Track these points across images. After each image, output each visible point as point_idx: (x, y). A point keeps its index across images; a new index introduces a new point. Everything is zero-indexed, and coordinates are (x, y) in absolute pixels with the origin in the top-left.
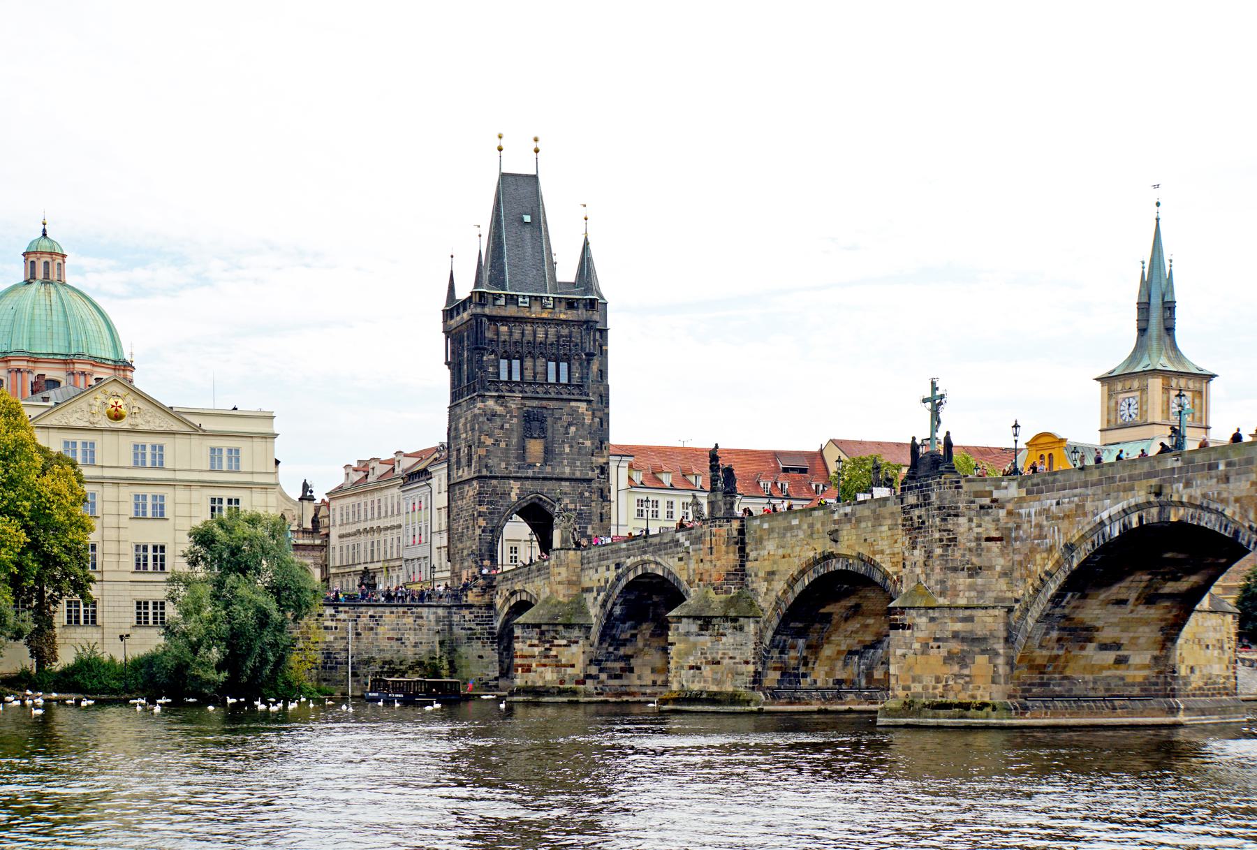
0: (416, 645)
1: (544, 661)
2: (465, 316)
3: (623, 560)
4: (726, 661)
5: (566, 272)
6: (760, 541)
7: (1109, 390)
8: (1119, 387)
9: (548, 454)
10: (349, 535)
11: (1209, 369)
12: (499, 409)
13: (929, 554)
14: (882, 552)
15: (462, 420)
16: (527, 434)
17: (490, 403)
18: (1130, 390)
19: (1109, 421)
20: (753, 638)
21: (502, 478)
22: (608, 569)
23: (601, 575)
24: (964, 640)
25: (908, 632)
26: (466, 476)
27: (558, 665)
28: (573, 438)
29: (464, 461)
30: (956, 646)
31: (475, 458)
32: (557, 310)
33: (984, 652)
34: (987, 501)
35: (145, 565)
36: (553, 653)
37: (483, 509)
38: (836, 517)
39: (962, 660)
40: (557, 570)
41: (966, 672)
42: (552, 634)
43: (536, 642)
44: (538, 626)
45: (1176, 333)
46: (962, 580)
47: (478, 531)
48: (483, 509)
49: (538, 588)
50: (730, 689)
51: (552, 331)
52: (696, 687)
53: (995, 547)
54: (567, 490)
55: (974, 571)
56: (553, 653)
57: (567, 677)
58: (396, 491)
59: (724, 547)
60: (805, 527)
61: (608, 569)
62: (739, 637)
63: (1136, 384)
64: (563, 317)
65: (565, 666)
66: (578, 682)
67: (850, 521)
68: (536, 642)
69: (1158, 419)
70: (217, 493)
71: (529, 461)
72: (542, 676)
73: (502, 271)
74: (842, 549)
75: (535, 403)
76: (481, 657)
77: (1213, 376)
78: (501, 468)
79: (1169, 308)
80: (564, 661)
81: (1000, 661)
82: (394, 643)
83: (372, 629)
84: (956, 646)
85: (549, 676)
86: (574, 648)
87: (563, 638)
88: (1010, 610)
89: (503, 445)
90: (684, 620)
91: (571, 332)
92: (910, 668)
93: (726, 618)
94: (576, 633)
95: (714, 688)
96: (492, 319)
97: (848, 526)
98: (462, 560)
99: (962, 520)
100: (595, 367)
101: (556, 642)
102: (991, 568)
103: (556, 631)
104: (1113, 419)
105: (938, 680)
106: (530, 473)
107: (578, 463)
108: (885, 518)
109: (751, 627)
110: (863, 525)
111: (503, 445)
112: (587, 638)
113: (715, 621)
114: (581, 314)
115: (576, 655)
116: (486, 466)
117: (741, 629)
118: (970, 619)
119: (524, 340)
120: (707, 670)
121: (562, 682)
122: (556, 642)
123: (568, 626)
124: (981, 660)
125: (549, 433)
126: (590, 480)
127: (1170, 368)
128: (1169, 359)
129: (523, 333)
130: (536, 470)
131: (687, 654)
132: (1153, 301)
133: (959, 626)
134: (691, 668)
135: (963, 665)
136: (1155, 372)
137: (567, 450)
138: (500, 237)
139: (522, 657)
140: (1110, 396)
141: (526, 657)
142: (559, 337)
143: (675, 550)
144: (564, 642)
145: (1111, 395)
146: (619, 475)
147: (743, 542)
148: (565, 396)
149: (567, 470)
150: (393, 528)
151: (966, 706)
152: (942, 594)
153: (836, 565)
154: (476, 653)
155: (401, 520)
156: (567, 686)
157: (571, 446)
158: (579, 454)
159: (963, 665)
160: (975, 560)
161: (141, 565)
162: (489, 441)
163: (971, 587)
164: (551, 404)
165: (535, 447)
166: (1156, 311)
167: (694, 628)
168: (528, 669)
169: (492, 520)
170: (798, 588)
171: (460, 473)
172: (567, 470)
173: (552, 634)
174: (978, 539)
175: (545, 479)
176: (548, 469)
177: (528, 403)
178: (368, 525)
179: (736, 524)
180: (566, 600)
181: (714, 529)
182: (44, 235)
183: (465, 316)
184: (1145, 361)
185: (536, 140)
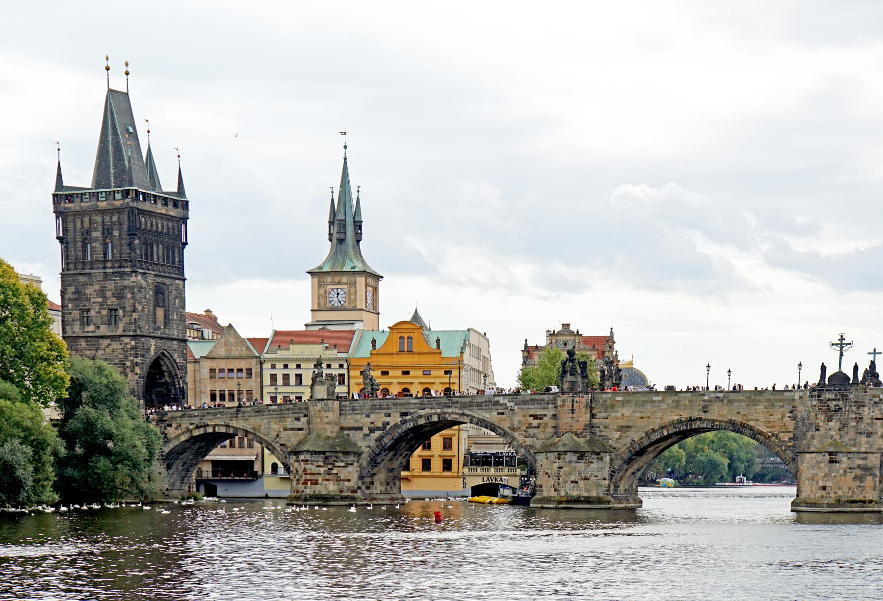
1: (327, 477)
3: (412, 411)
4: (593, 478)
7: (319, 282)
8: (329, 280)
13: (844, 425)
14: (757, 420)
15: (97, 287)
16: (157, 305)
18: (339, 283)
19: (319, 304)
20: (608, 465)
24: (862, 469)
27: (338, 480)
30: (858, 472)
34: (877, 400)
36: (334, 471)
37: (138, 360)
38: (706, 398)
39: (859, 478)
40: (324, 414)
41: (862, 485)
42: (334, 458)
44: (323, 453)
46: (864, 439)
47: (137, 377)
48: (138, 360)
50: (595, 495)
52: (575, 493)
53: (879, 422)
54: (176, 347)
55: (869, 435)
56: (334, 471)
57: (345, 488)
59: (584, 410)
60: (670, 402)
62: (601, 464)
63: (345, 279)
65: (343, 480)
66: (353, 492)
67: (722, 401)
68: (322, 464)
69: (364, 308)
72: (326, 487)
77: (382, 277)
78: (146, 329)
80: (342, 477)
81: (877, 479)
84: (858, 472)
85: (332, 488)
86: (350, 468)
87: (342, 461)
89: (146, 310)
90: (569, 454)
92: (838, 483)
93: (593, 452)
94: (351, 458)
95: (586, 494)
97: (720, 404)
101: (336, 464)
102: (876, 433)
103: (337, 457)
104: (322, 302)
105: (850, 489)
108: (760, 401)
109: (607, 458)
110: (735, 404)
111: (146, 310)
113: (586, 454)
115: (351, 473)
117: (602, 459)
118: (865, 458)
120: (581, 483)
121: (341, 491)
123: (346, 453)
124: (869, 478)
131: (570, 474)
132: (348, 220)
134: (572, 482)
135: (861, 482)
136: (363, 273)
137: (175, 317)
138: (107, 137)
140: (320, 286)
141: (314, 474)
145: (320, 285)
151: (864, 502)
152: (854, 445)
156: (345, 494)
159: (861, 482)
160: (870, 429)
163: (867, 443)
165: (160, 312)
166: (345, 226)
167: (574, 458)
168: (315, 483)
171: (91, 328)
172: (176, 332)
173: (334, 458)
174: (872, 419)
175: (167, 339)
176: (167, 331)
180: (334, 435)
181: (576, 399)
185: (127, 64)
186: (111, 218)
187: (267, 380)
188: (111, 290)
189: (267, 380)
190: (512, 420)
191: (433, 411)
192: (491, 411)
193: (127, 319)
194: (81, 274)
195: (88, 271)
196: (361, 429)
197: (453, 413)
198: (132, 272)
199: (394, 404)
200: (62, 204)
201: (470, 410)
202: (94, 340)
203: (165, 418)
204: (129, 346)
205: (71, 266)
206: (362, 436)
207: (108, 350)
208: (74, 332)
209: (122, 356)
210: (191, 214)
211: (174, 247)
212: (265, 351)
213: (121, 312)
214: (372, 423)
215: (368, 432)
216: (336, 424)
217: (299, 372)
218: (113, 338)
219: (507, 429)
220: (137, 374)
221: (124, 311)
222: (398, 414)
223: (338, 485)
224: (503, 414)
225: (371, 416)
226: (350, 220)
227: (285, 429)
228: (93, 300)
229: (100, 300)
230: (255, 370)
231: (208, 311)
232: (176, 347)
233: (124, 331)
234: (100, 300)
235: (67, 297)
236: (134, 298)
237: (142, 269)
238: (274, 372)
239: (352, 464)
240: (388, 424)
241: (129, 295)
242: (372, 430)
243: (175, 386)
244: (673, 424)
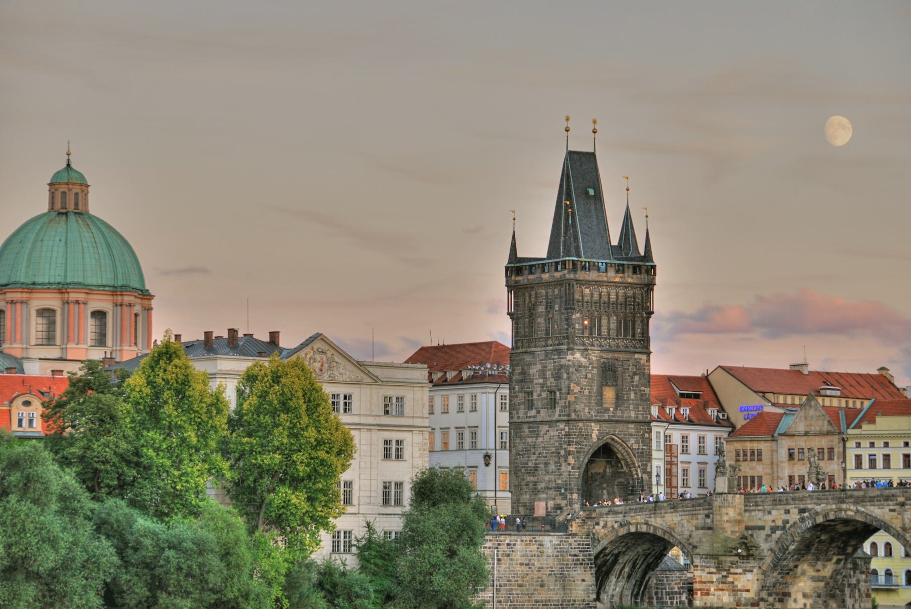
0: (540, 569)
3: (810, 506)
9: (619, 399)
15: (539, 367)
17: (578, 355)
22: (787, 512)
28: (637, 386)
32: (626, 274)
36: (730, 579)
37: (572, 448)
43: (714, 570)
47: (570, 468)
48: (572, 448)
51: (621, 292)
54: (633, 431)
56: (730, 579)
64: (630, 280)
65: (741, 591)
71: (605, 406)
75: (610, 355)
76: (583, 580)
82: (525, 568)
83: (508, 555)
86: (749, 576)
91: (634, 294)
94: (752, 563)
98: (535, 491)
101: (732, 570)
106: (606, 417)
107: (641, 409)
111: (586, 392)
112: (760, 567)
116: (575, 411)
122: (732, 570)
125: (620, 383)
129: (600, 295)
130: (611, 414)
137: (633, 396)
139: (701, 582)
141: (705, 583)
142: (626, 298)
143: (885, 503)
144: (740, 571)
148: (632, 349)
149: (633, 414)
154: (580, 578)
157: (635, 393)
158: (641, 400)
162: (577, 389)
164: (621, 356)
165: (609, 394)
169: (578, 458)
171: (533, 413)
172: (633, 414)
175: (617, 421)
176: (619, 413)
177: (604, 355)
182: (68, 165)
186: (553, 291)
187: (851, 463)
188: (550, 370)
189: (851, 463)
190: (903, 519)
191: (829, 507)
192: (881, 507)
193: (563, 401)
194: (526, 352)
195: (533, 349)
196: (763, 528)
197: (850, 510)
198: (568, 349)
199: (794, 499)
200: (513, 278)
201: (863, 506)
202: (534, 425)
203: (593, 515)
204: (563, 433)
205: (520, 344)
206: (764, 537)
207: (546, 437)
208: (519, 417)
209: (557, 444)
210: (658, 279)
211: (634, 317)
212: (853, 425)
213: (558, 393)
214: (773, 521)
215: (769, 532)
216: (739, 522)
217: (886, 451)
218: (551, 423)
219: (899, 529)
220: (569, 464)
221: (560, 394)
222: (796, 511)
223: (734, 595)
224: (894, 510)
225: (773, 512)
227: (697, 529)
228: (535, 381)
229: (541, 381)
230: (838, 449)
231: (883, 369)
232: (633, 431)
233: (560, 415)
234: (541, 381)
235: (514, 378)
236: (568, 378)
237: (584, 344)
238: (858, 452)
239: (752, 571)
240: (788, 522)
241: (565, 376)
242: (774, 529)
243: (632, 476)
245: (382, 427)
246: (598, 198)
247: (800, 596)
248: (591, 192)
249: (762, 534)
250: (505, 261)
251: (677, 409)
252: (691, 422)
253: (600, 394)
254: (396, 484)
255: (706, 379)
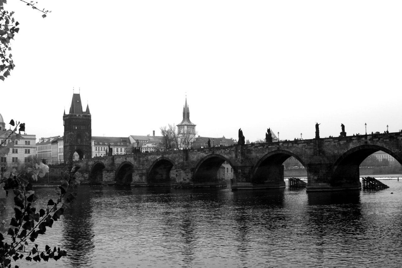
2: (67, 118)
5: (84, 110)
6: (116, 159)
9: (82, 141)
10: (40, 152)
11: (195, 124)
12: (73, 134)
13: (137, 163)
17: (72, 133)
21: (74, 145)
23: (91, 163)
25: (134, 173)
26: (67, 145)
29: (67, 142)
31: (69, 142)
33: (144, 175)
35: (14, 161)
37: (70, 151)
45: (190, 118)
46: (141, 166)
49: (81, 164)
51: (82, 120)
53: (145, 162)
54: (84, 147)
58: (50, 145)
59: (110, 160)
61: (92, 162)
63: (183, 127)
64: (84, 118)
70: (26, 149)
73: (74, 110)
74: (127, 161)
79: (188, 114)
82: (56, 174)
86: (87, 175)
88: (147, 170)
96: (73, 119)
98: (66, 159)
99: (141, 158)
100: (89, 126)
102: (145, 164)
107: (86, 143)
112: (89, 173)
114: (87, 118)
119: (77, 122)
126: (88, 146)
127: (188, 124)
128: (188, 122)
133: (141, 172)
136: (186, 125)
140: (179, 128)
145: (179, 128)
146: (93, 143)
147: (113, 159)
149: (85, 144)
150: (49, 151)
152: (139, 168)
153: (126, 163)
155: (52, 150)
161: (13, 161)
165: (79, 140)
166: (186, 114)
167: (106, 172)
170: (121, 166)
174: (143, 161)
178: (44, 151)
179: (112, 157)
183: (67, 118)
184: (184, 123)
226: (186, 112)
244: (123, 163)
245: (24, 147)
246: (80, 102)
247: (99, 178)
248: (78, 101)
249: (90, 166)
250: (63, 115)
251: (120, 144)
252: (123, 146)
253: (77, 140)
254: (16, 158)
255: (129, 138)
